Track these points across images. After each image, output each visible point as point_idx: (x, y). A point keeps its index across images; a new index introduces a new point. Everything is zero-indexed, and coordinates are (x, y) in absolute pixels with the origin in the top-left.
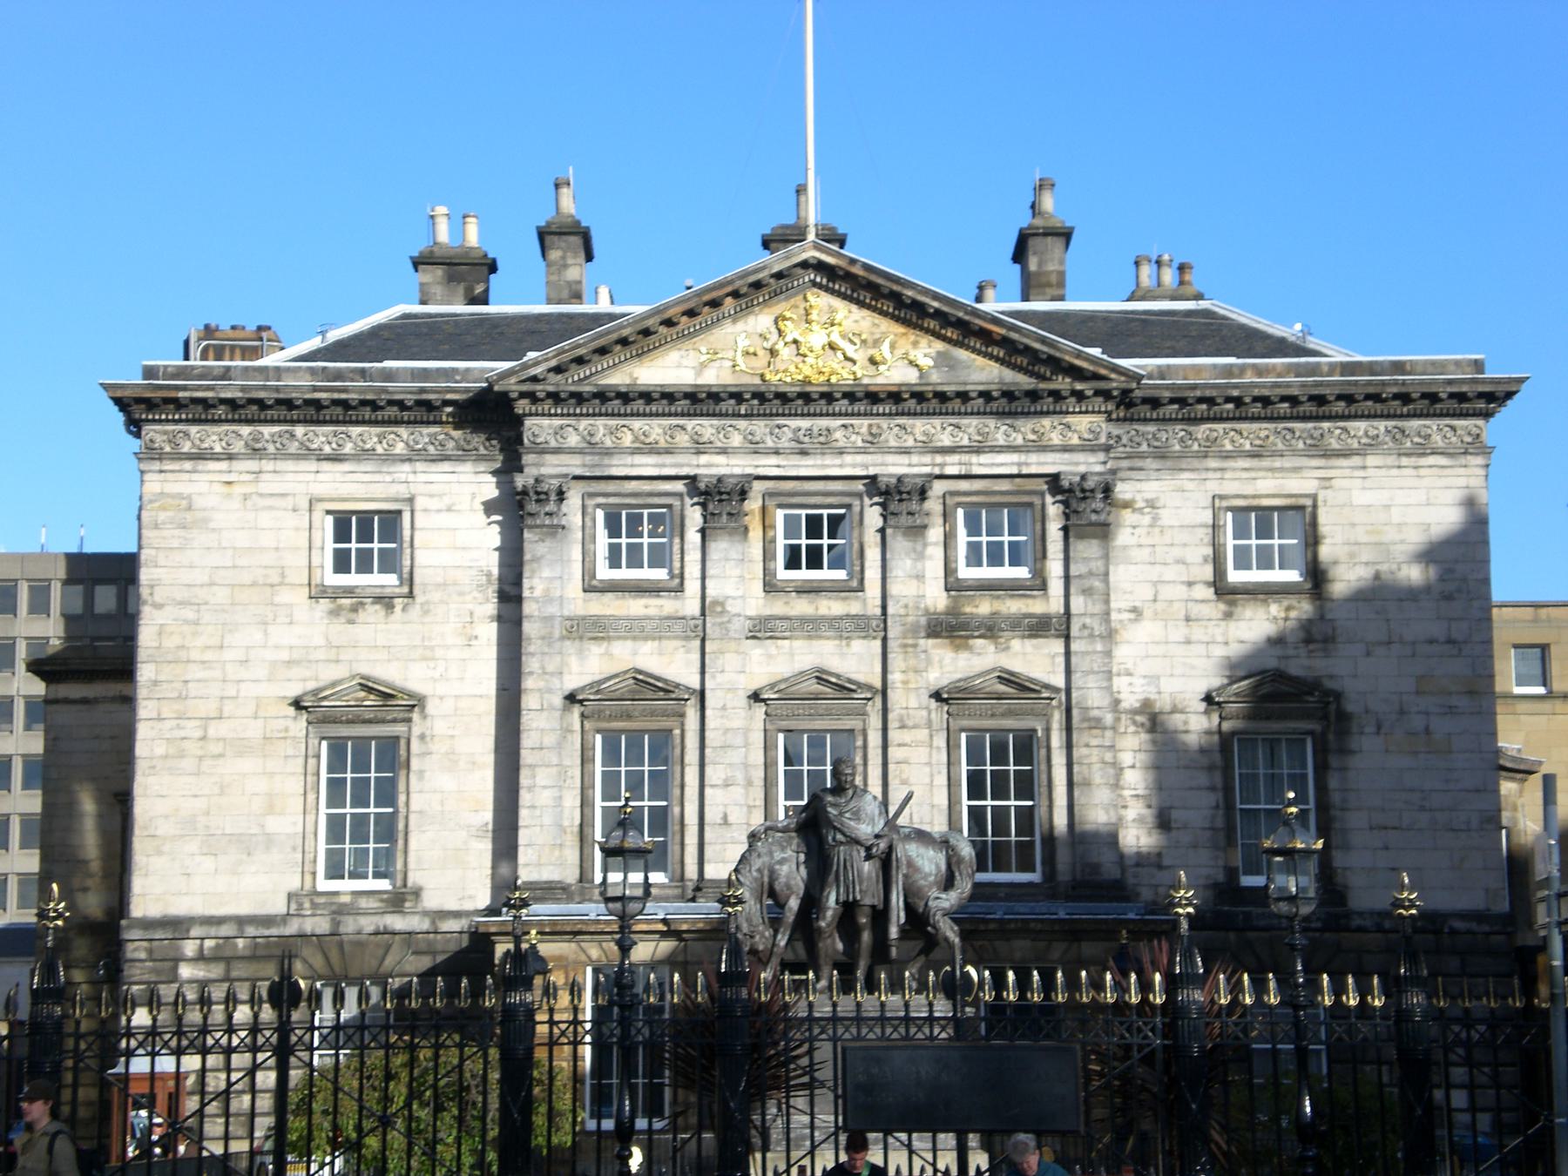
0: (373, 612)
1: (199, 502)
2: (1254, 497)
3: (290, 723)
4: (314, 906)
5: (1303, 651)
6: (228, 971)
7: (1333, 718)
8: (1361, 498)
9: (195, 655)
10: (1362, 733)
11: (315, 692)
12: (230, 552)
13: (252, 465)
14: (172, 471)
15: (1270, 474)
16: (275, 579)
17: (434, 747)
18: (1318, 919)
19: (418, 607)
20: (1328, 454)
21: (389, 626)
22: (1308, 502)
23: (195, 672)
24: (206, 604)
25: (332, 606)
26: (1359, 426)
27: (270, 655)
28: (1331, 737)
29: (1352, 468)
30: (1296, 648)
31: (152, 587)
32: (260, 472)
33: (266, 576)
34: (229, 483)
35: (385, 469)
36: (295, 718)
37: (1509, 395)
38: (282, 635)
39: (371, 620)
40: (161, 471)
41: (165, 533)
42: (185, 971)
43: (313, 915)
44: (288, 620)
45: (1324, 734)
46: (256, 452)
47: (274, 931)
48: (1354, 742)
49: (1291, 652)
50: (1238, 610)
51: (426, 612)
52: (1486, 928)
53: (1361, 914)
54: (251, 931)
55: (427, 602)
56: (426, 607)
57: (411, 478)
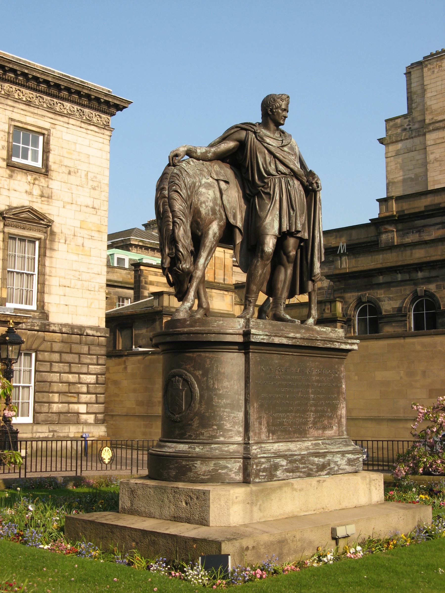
2: (26, 124)
5: (39, 200)
7: (49, 233)
8: (67, 137)
10: (59, 242)
15: (32, 115)
18: (38, 325)
20: (56, 113)
22: (46, 132)
26: (68, 105)
28: (47, 242)
29: (63, 122)
30: (37, 198)
37: (125, 107)
45: (45, 240)
48: (56, 246)
49: (35, 200)
50: (15, 175)
52: (99, 334)
53: (54, 324)
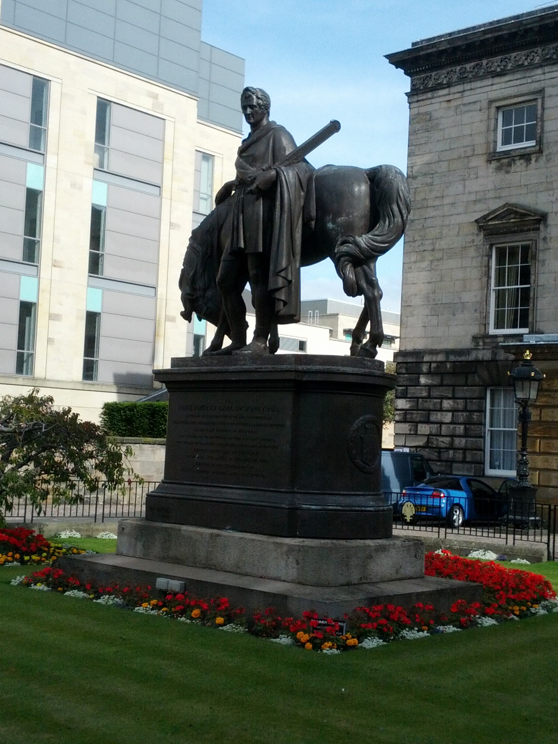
0: (520, 164)
1: (436, 115)
3: (475, 237)
4: (485, 344)
6: (442, 380)
9: (431, 203)
11: (484, 217)
12: (448, 141)
13: (459, 88)
14: (423, 100)
16: (470, 153)
17: (551, 245)
19: (544, 158)
21: (528, 172)
23: (431, 213)
24: (436, 173)
25: (498, 164)
27: (465, 198)
31: (412, 167)
32: (464, 91)
33: (465, 152)
34: (449, 101)
35: (528, 75)
36: (478, 235)
38: (474, 186)
39: (519, 170)
40: (418, 101)
41: (419, 136)
42: (423, 380)
43: (483, 349)
44: (475, 176)
46: (462, 80)
47: (463, 358)
51: (548, 160)
54: (452, 358)
55: (550, 154)
56: (549, 157)
57: (542, 77)
